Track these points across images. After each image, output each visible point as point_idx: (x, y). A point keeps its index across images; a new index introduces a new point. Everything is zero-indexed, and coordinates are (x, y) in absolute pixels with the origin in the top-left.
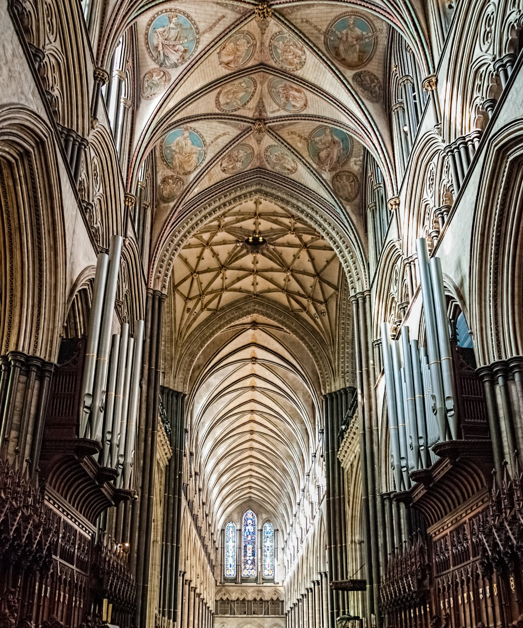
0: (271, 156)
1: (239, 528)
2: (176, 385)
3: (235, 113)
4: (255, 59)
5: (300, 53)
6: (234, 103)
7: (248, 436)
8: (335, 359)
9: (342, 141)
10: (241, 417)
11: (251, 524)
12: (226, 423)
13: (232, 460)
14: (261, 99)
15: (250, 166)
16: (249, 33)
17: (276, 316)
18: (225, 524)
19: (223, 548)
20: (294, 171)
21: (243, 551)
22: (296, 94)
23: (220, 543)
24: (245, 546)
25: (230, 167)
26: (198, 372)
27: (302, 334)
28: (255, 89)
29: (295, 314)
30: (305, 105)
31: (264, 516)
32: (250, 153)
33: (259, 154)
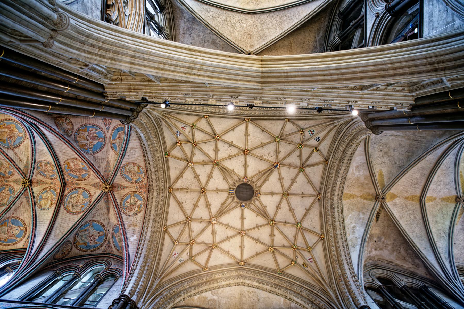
0: (135, 179)
3: (92, 203)
4: (58, 188)
5: (43, 164)
6: (85, 202)
9: (119, 132)
14: (92, 185)
15: (144, 194)
16: (42, 191)
20: (137, 165)
22: (72, 165)
25: (137, 209)
28: (82, 188)
30: (76, 159)
32: (133, 194)
33: (137, 188)
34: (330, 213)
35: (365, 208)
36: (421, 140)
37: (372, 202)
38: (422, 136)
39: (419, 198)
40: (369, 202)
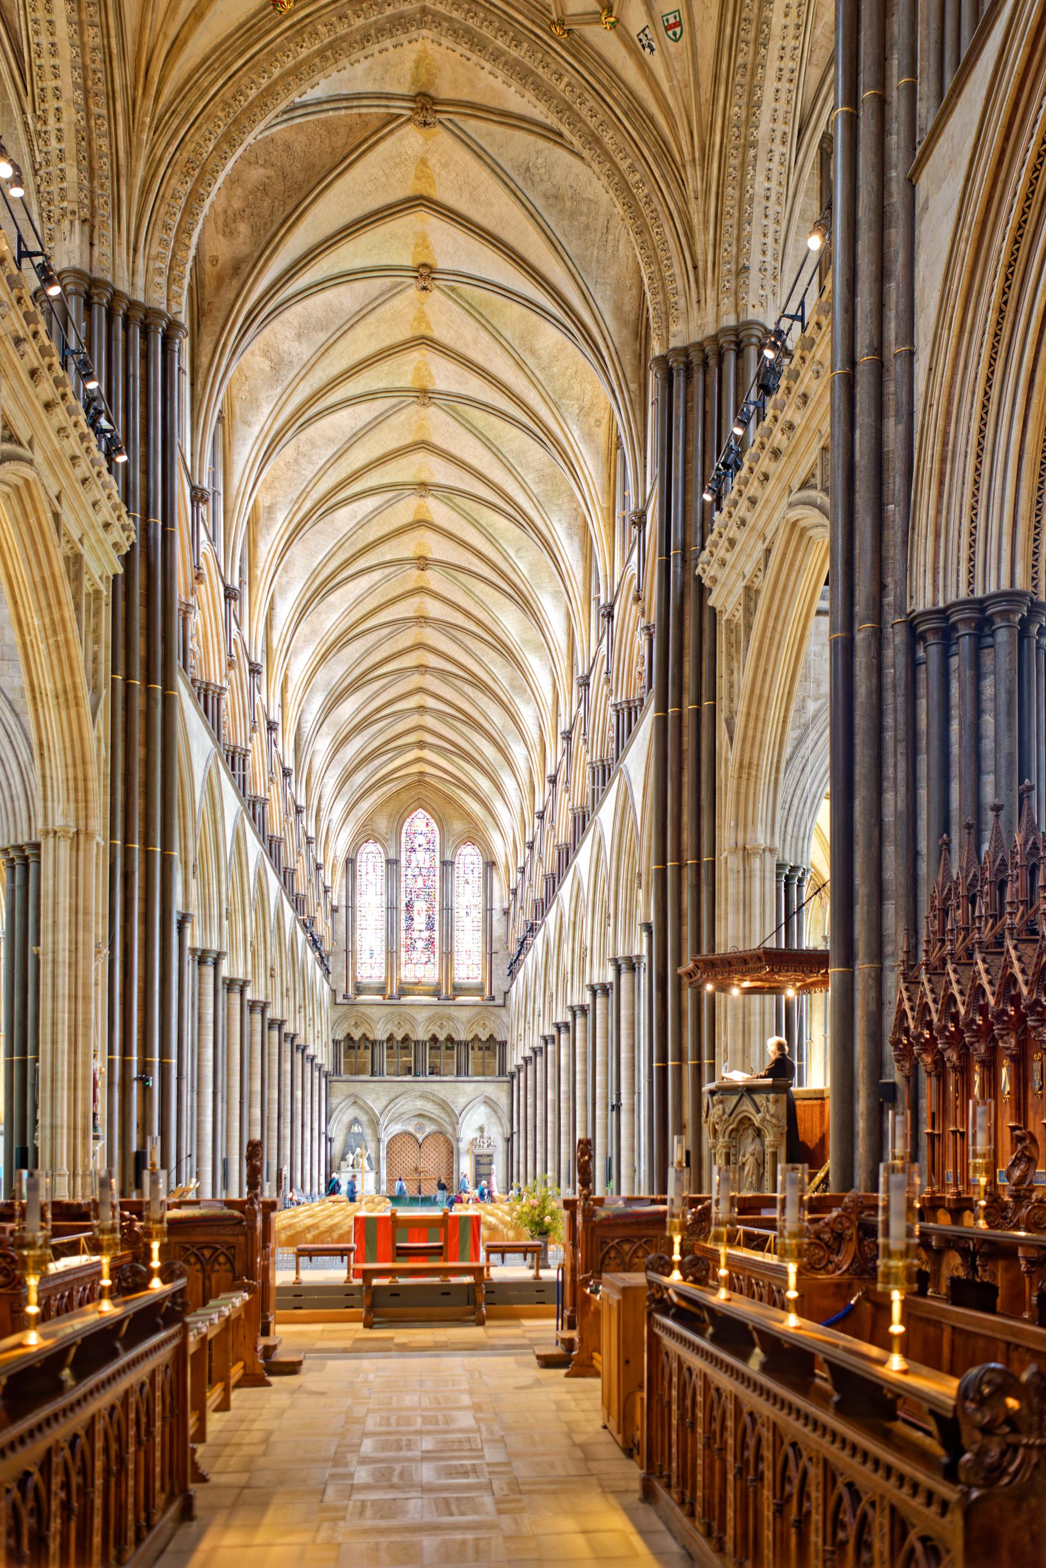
1: (392, 855)
2: (140, 281)
7: (412, 577)
8: (706, 222)
10: (389, 504)
11: (425, 846)
12: (345, 518)
13: (368, 652)
17: (499, 43)
18: (355, 846)
19: (351, 907)
21: (403, 916)
23: (344, 894)
24: (409, 906)
26: (236, 283)
27: (592, 123)
29: (569, 32)
31: (458, 826)
34: (373, 19)
35: (386, 71)
36: (610, 244)
37: (407, 84)
38: (621, 247)
39: (425, 194)
40: (408, 77)
